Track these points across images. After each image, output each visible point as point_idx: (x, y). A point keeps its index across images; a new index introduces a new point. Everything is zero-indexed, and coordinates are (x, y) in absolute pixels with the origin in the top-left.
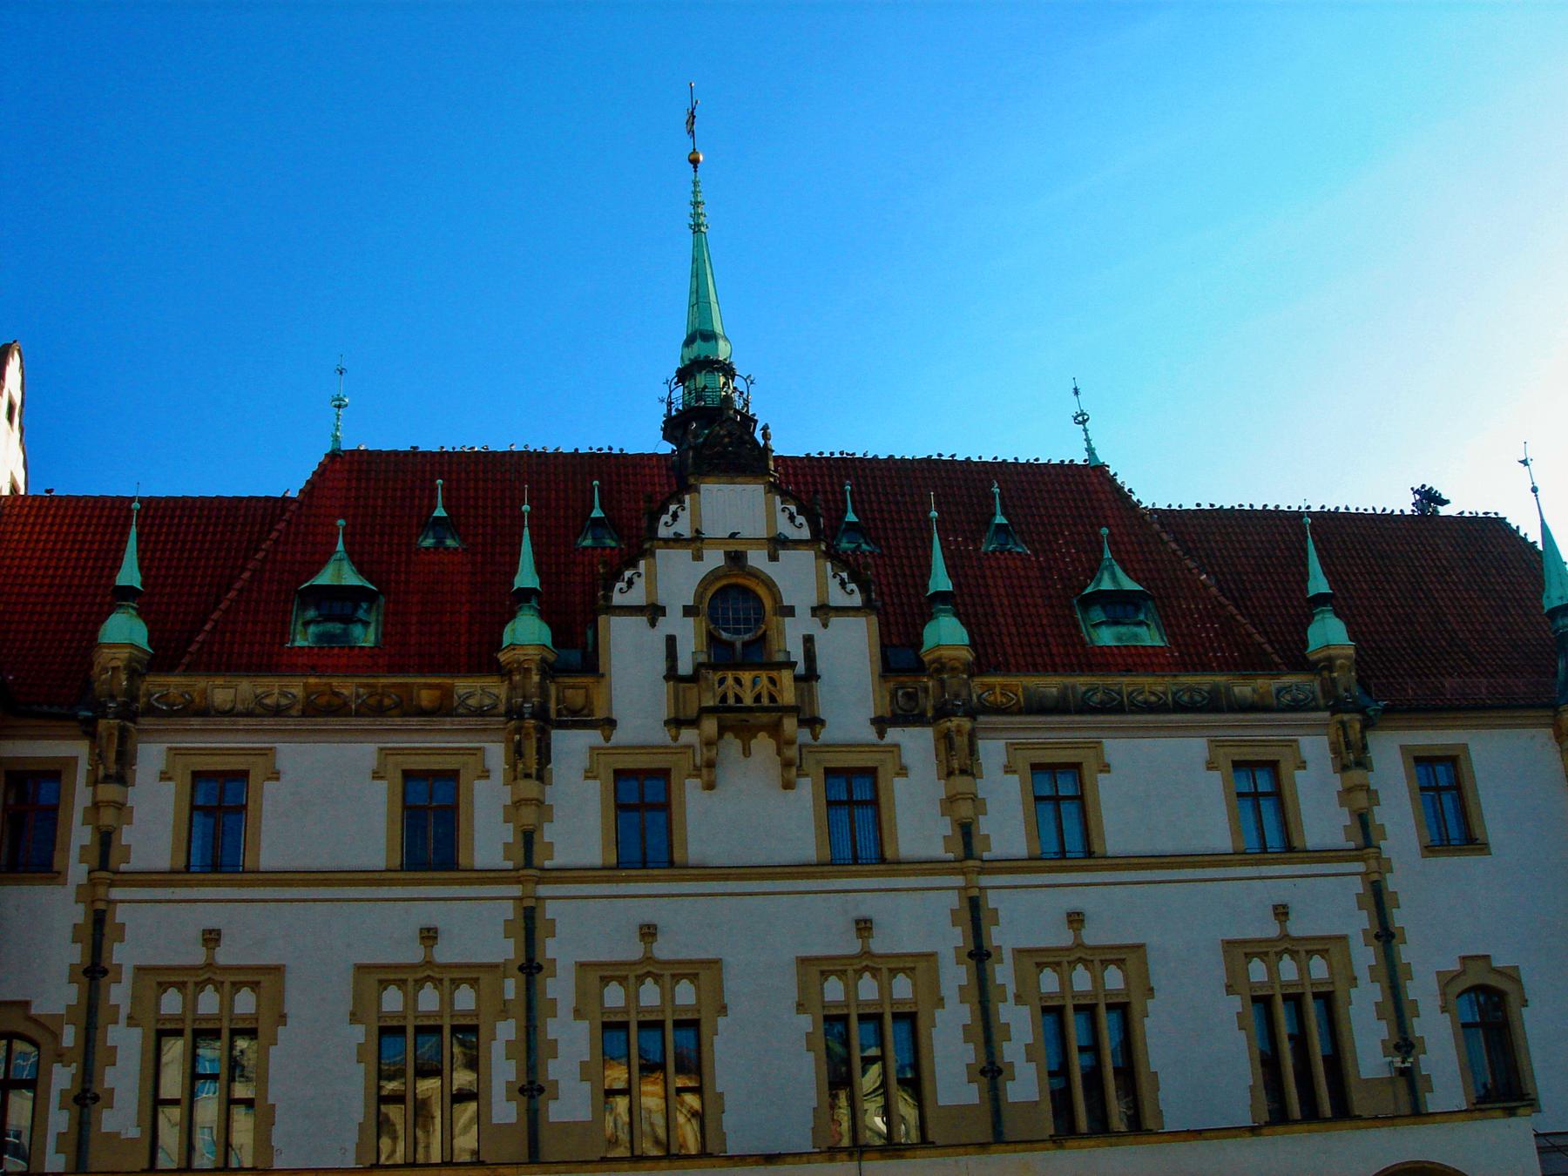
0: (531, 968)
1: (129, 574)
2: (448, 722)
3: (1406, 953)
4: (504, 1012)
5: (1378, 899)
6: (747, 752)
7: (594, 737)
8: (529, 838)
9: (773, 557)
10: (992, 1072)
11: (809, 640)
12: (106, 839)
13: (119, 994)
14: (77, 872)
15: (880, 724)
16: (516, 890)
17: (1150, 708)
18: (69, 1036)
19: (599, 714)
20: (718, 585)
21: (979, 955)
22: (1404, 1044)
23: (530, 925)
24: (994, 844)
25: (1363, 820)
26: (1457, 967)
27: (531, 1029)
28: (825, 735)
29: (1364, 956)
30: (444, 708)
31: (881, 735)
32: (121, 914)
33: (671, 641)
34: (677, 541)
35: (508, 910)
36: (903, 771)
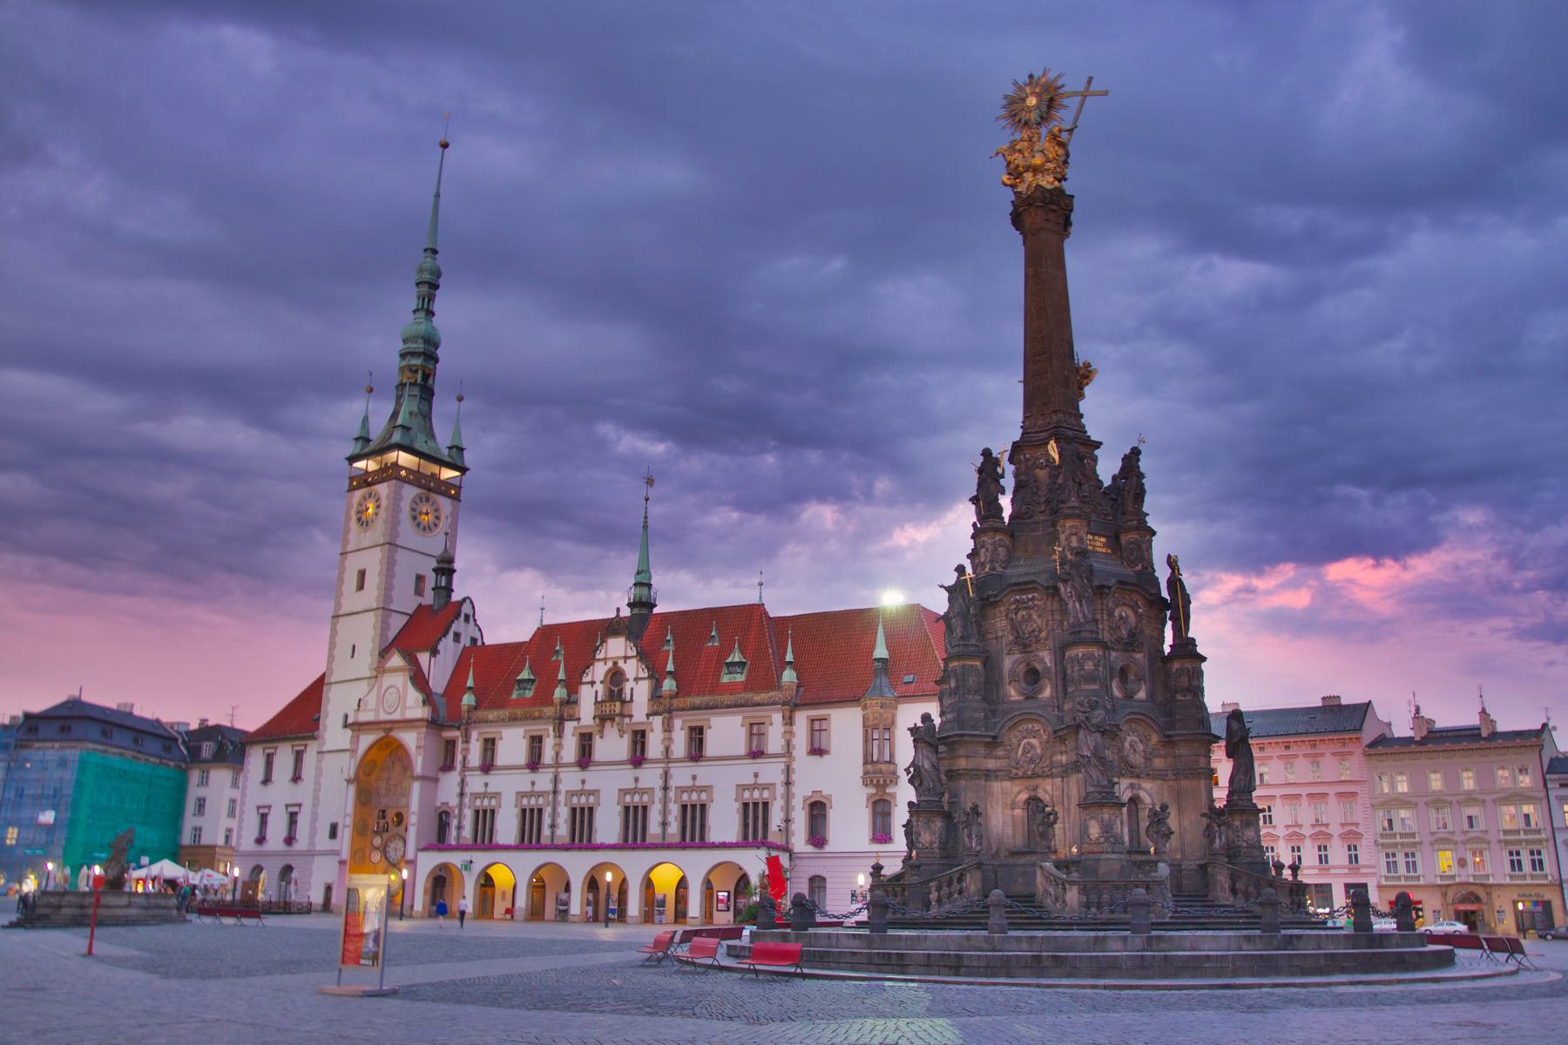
0: (555, 792)
1: (470, 683)
2: (539, 721)
3: (794, 789)
4: (548, 805)
5: (788, 771)
6: (612, 727)
7: (575, 723)
8: (557, 754)
9: (625, 662)
10: (664, 824)
11: (632, 689)
12: (465, 758)
13: (467, 800)
14: (458, 766)
15: (648, 716)
16: (553, 770)
17: (728, 707)
18: (456, 812)
19: (577, 716)
20: (610, 674)
21: (666, 788)
22: (788, 820)
23: (556, 780)
24: (675, 753)
25: (788, 744)
26: (810, 794)
27: (554, 810)
28: (634, 720)
29: (780, 790)
30: (540, 718)
31: (648, 719)
32: (468, 779)
33: (596, 692)
34: (599, 660)
35: (551, 776)
36: (652, 730)
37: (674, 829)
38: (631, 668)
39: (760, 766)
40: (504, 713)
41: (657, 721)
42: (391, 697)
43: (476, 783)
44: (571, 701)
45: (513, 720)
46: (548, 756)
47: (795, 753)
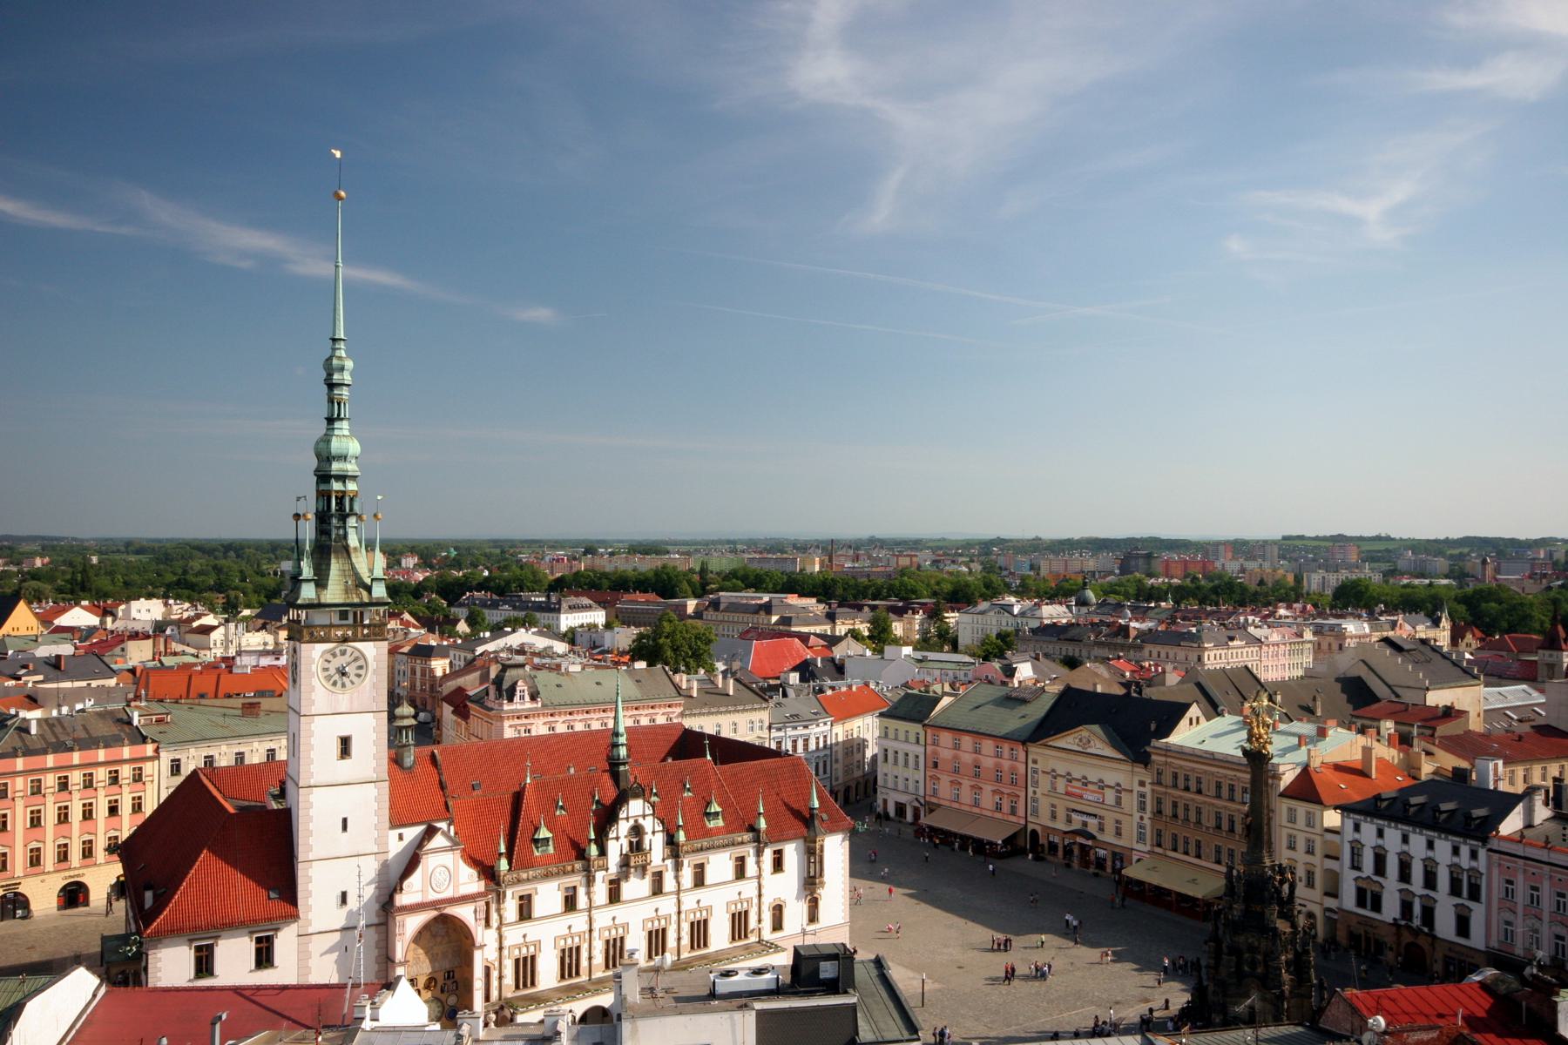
3: (763, 899)
7: (604, 873)
15: (664, 860)
18: (497, 964)
21: (679, 913)
37: (686, 941)
38: (648, 824)
39: (741, 885)
40: (539, 871)
41: (669, 862)
42: (441, 876)
43: (513, 936)
44: (603, 852)
45: (547, 876)
46: (582, 901)
47: (764, 874)
